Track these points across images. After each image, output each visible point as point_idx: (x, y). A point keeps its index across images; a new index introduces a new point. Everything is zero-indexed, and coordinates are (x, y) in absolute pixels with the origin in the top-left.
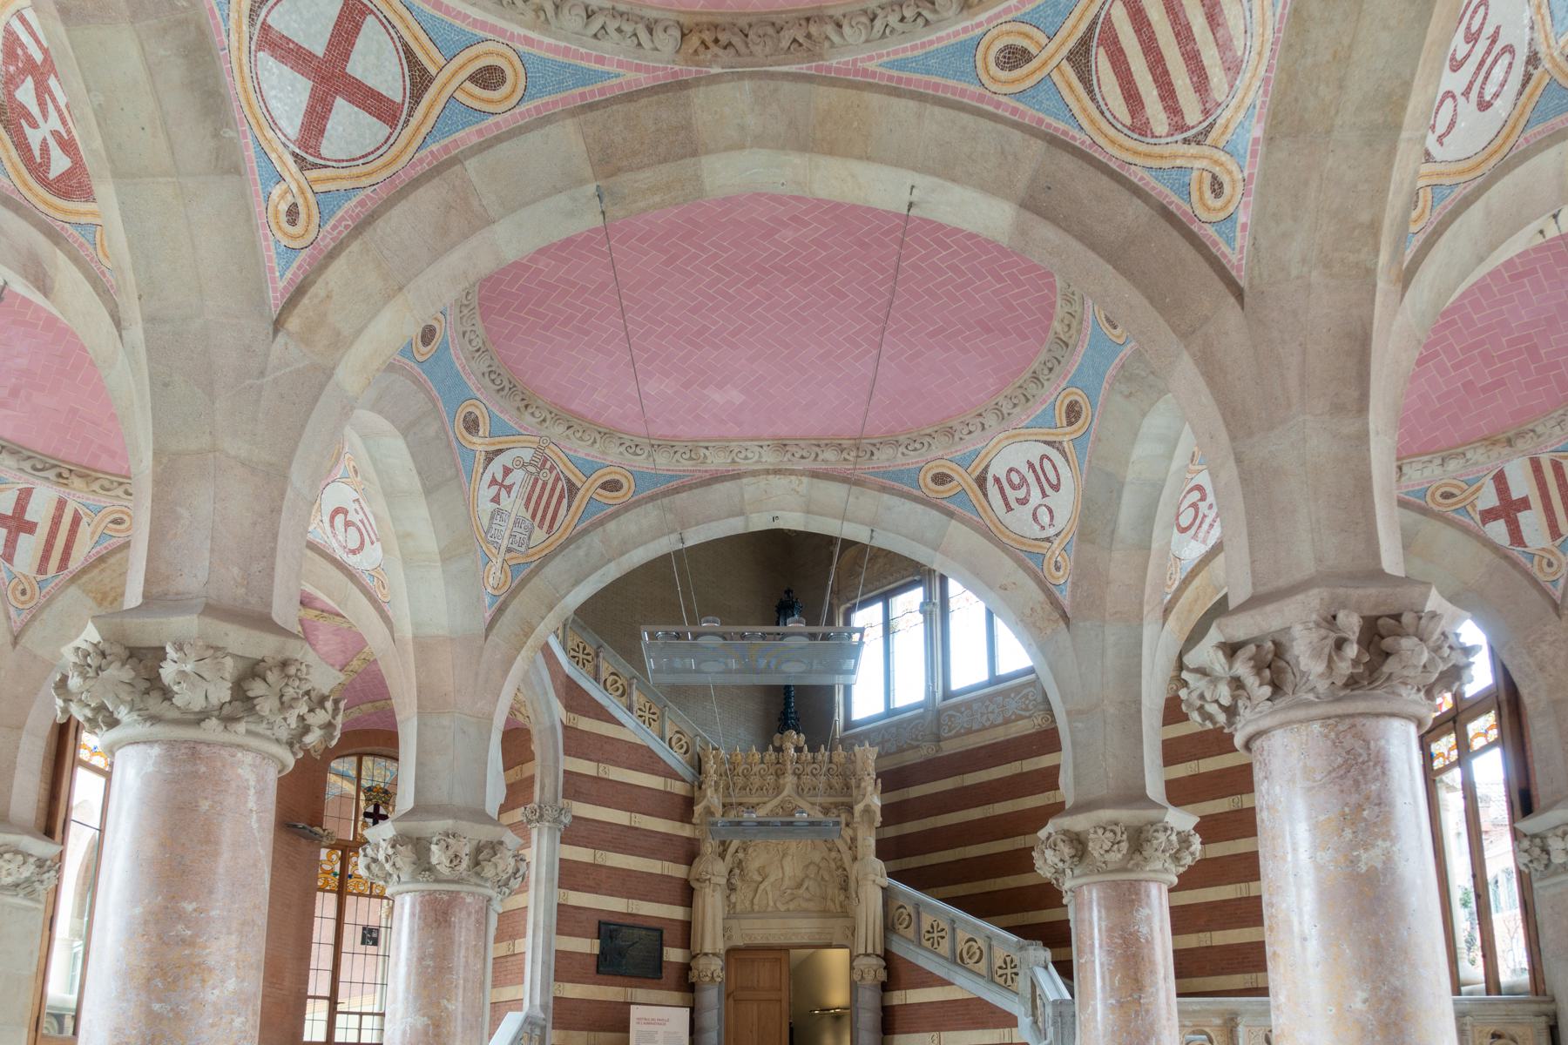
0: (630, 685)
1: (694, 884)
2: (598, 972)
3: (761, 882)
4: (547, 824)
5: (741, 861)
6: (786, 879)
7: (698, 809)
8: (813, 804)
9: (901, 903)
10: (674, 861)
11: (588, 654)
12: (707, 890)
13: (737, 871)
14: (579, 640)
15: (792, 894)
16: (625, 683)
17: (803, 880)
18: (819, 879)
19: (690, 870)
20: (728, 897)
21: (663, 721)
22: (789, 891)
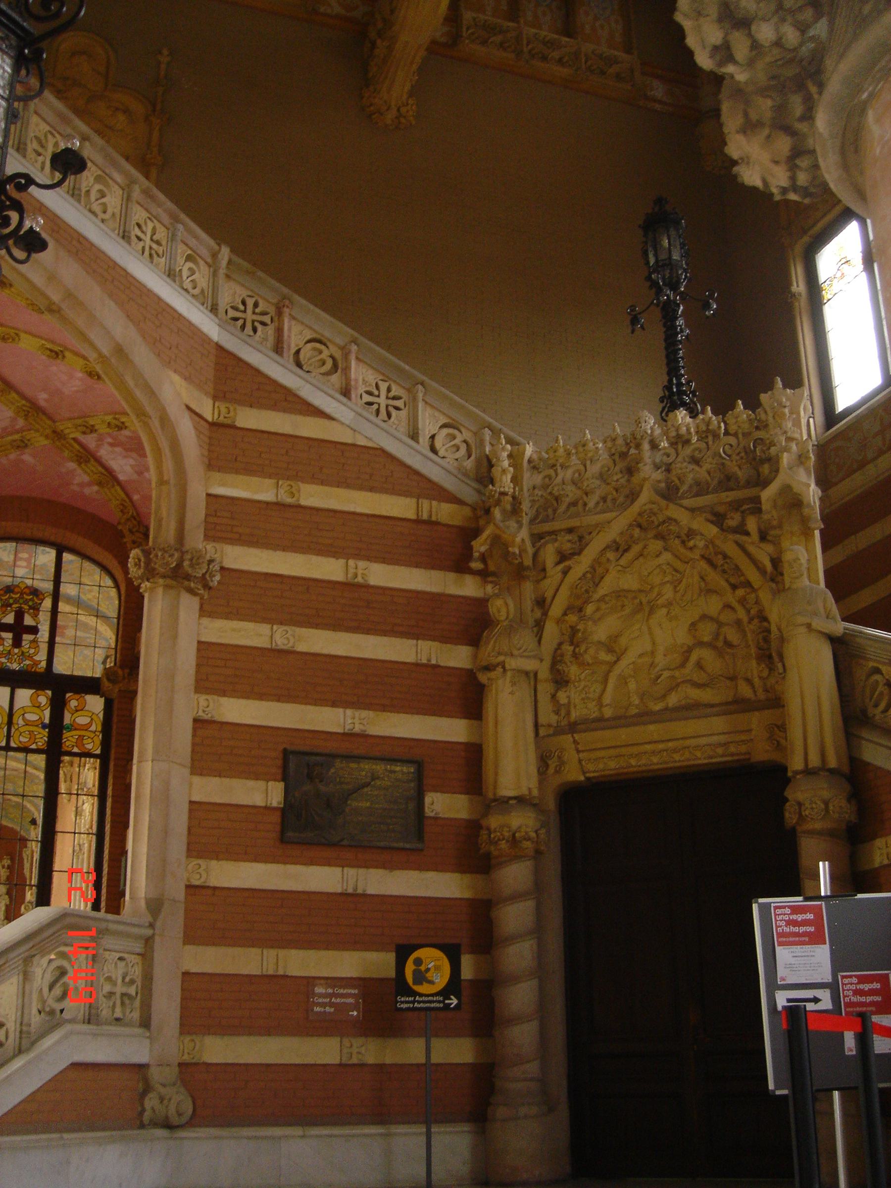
0: (346, 356)
1: (483, 678)
2: (283, 840)
3: (615, 662)
4: (161, 581)
5: (574, 630)
6: (661, 650)
7: (480, 546)
8: (692, 510)
9: (871, 664)
10: (444, 639)
11: (264, 314)
12: (500, 682)
13: (568, 649)
14: (244, 293)
15: (673, 677)
16: (338, 355)
17: (689, 650)
18: (720, 644)
19: (475, 656)
20: (554, 696)
21: (416, 408)
22: (666, 674)
